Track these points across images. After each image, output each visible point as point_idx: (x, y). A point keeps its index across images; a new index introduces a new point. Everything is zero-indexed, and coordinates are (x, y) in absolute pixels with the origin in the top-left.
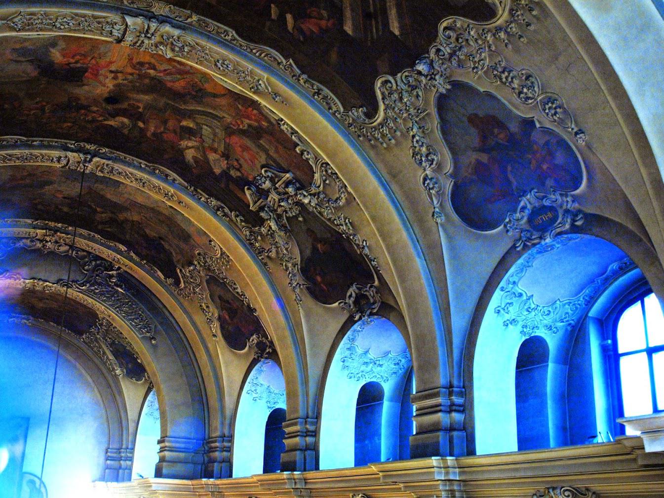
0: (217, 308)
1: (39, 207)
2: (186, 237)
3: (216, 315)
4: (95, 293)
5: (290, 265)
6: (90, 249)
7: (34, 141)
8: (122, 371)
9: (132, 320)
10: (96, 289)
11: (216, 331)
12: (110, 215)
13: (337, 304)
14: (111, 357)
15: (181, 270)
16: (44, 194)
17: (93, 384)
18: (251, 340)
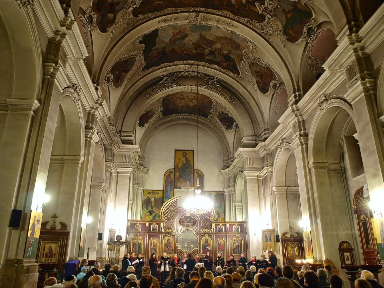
0: (255, 78)
1: (185, 52)
2: (238, 47)
3: (255, 81)
4: (209, 88)
5: (278, 32)
6: (206, 72)
7: (178, 10)
8: (224, 127)
9: (225, 96)
10: (210, 86)
11: (256, 89)
12: (210, 49)
13: (300, 40)
14: (220, 123)
15: (239, 66)
16: (185, 43)
17: (214, 137)
18: (270, 86)
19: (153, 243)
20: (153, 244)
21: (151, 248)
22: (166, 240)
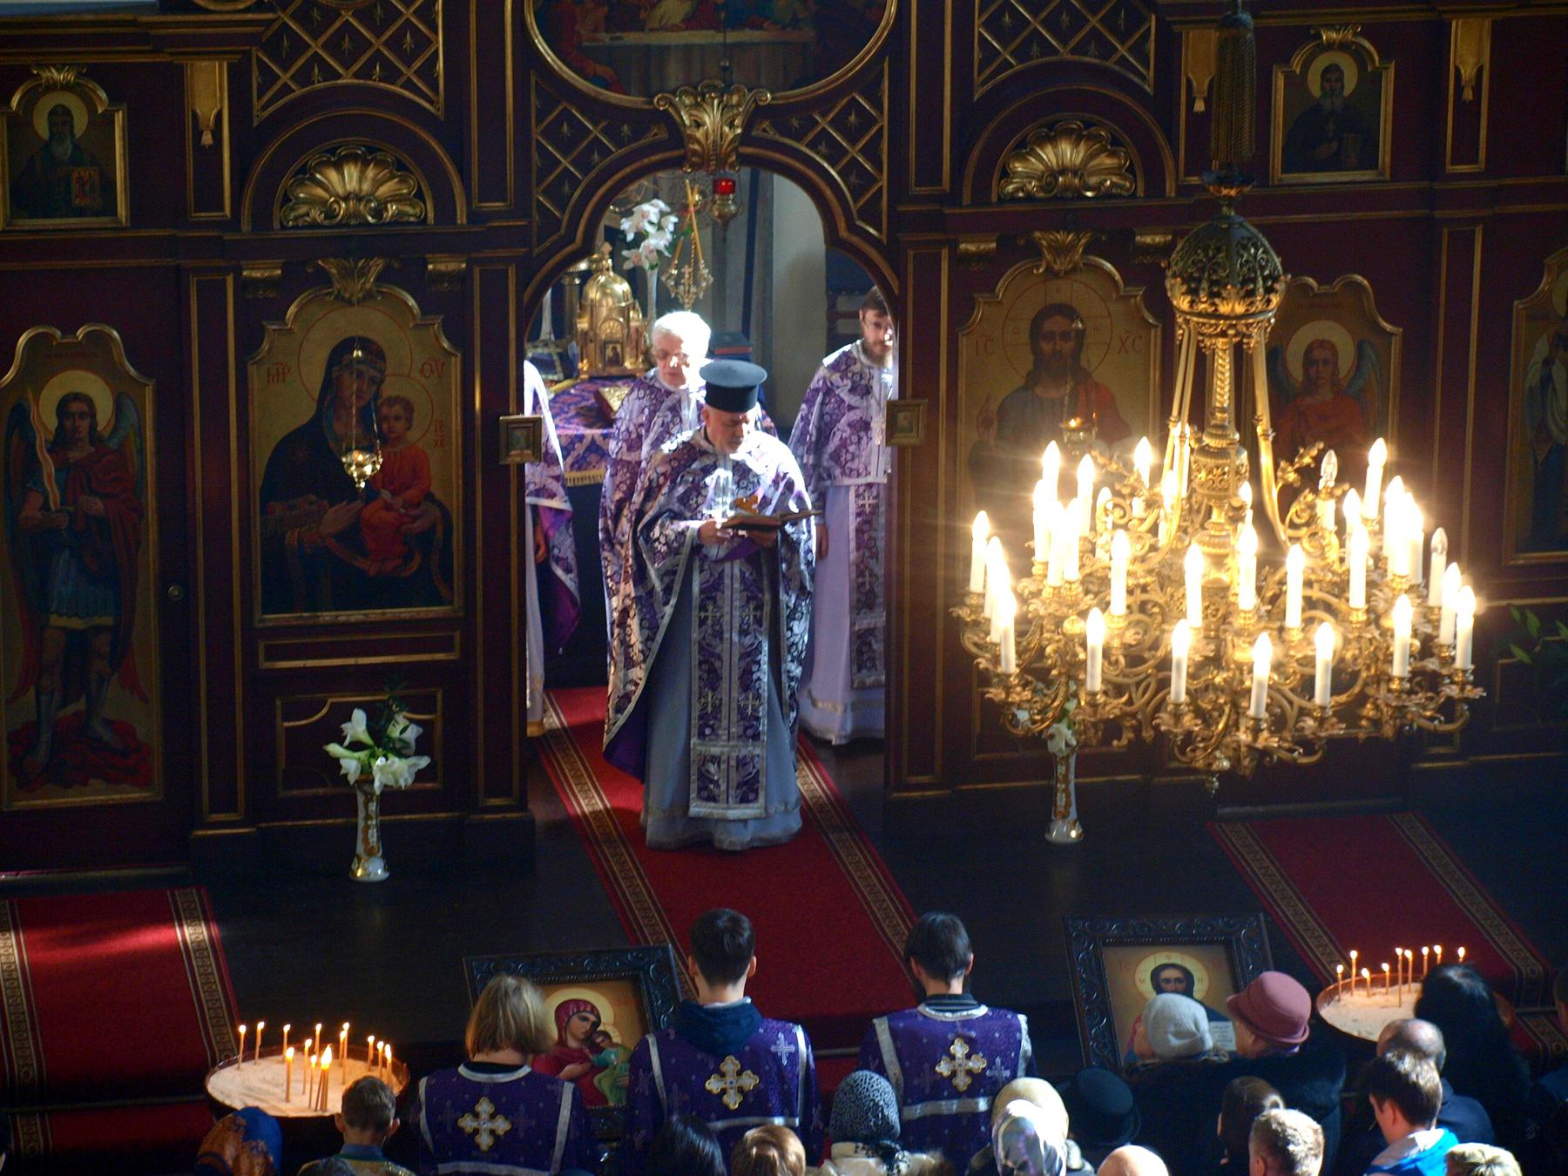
19: (45, 416)
20: (62, 441)
21: (31, 511)
22: (313, 373)
